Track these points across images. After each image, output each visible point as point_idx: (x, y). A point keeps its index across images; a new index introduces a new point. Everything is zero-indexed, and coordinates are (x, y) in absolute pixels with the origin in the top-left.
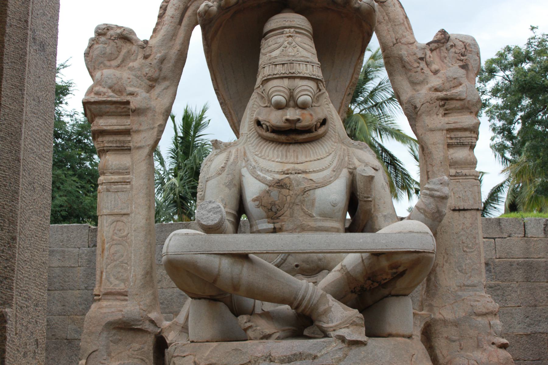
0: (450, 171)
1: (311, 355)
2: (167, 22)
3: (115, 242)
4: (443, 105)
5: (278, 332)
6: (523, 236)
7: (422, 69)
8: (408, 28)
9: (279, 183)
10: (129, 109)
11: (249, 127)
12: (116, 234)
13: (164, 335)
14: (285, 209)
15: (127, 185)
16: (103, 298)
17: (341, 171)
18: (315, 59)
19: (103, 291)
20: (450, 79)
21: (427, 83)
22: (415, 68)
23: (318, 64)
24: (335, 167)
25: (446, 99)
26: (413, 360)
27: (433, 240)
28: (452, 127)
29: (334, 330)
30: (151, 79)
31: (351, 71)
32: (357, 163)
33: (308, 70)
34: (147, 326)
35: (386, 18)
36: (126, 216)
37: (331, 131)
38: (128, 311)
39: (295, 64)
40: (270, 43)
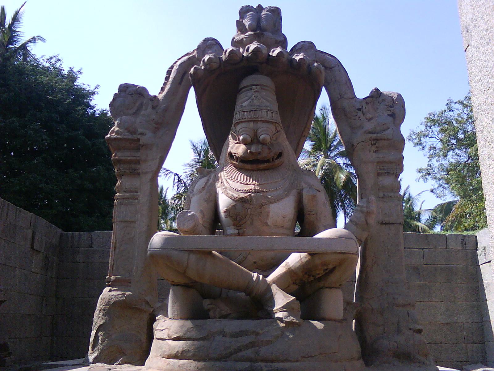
4: (375, 144)
6: (445, 247)
7: (359, 117)
10: (139, 145)
14: (247, 219)
18: (276, 108)
23: (277, 112)
30: (156, 123)
32: (304, 185)
33: (269, 117)
39: (258, 111)
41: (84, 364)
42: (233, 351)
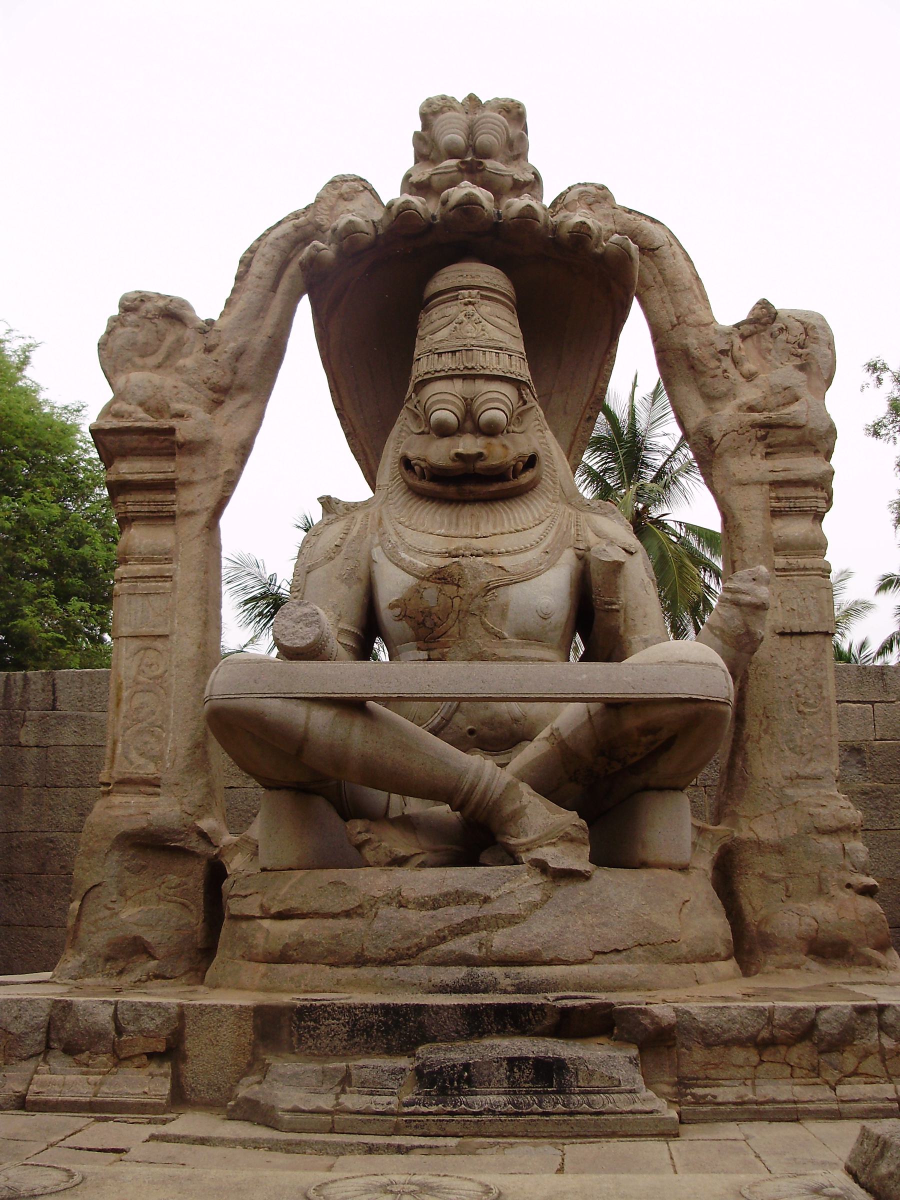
0: (776, 560)
1: (477, 895)
2: (250, 286)
3: (140, 687)
5: (423, 853)
8: (700, 297)
9: (439, 573)
10: (173, 442)
11: (393, 473)
12: (144, 672)
13: (225, 860)
14: (450, 622)
15: (166, 581)
16: (115, 788)
17: (561, 553)
19: (116, 776)
20: (777, 391)
21: (735, 396)
22: (712, 369)
23: (522, 353)
24: (548, 546)
25: (768, 426)
26: (685, 911)
27: (726, 678)
28: (780, 479)
29: (528, 850)
30: (215, 389)
31: (593, 375)
32: (592, 539)
33: (501, 363)
34: (194, 843)
35: (659, 279)
36: (162, 640)
37: (546, 481)
38: (159, 814)
40: (434, 317)
41: (54, 979)
42: (424, 940)
